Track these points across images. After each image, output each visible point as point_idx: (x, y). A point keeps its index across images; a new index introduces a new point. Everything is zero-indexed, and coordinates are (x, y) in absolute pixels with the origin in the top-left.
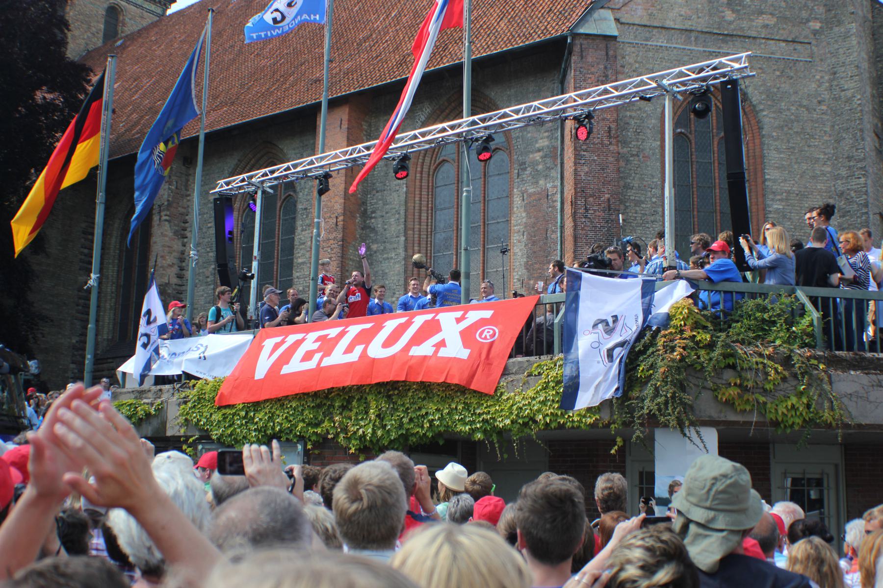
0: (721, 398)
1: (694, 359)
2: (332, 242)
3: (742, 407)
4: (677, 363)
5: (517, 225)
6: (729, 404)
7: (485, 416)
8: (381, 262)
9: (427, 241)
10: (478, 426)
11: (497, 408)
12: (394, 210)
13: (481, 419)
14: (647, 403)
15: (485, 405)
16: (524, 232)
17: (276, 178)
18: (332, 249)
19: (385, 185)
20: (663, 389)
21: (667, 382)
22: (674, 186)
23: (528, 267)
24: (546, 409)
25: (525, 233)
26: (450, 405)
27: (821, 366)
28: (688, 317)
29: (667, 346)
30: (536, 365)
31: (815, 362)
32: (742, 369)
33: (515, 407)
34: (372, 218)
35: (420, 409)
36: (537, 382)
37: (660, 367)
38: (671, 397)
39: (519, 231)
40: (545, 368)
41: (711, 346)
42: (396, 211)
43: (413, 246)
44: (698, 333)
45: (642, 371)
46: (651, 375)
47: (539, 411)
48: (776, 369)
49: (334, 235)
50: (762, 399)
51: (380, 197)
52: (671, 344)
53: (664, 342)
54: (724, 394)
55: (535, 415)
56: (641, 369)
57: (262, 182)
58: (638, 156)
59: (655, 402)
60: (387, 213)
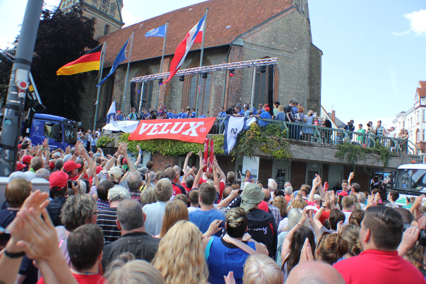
3: (266, 152)
6: (263, 151)
14: (242, 149)
17: (148, 79)
23: (214, 105)
27: (288, 143)
31: (286, 142)
35: (182, 145)
41: (260, 135)
48: (276, 143)
50: (272, 150)
57: (144, 80)
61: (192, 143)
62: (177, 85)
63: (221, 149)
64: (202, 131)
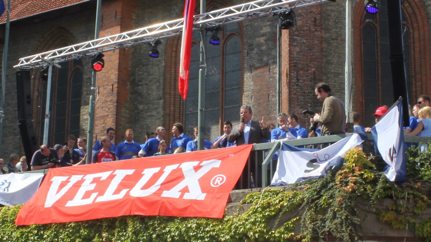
0: (382, 220)
1: (362, 191)
2: (109, 103)
3: (397, 226)
4: (349, 194)
5: (246, 91)
6: (389, 224)
7: (211, 233)
8: (146, 118)
9: (180, 103)
10: (206, 240)
11: (220, 227)
12: (156, 80)
13: (208, 235)
14: (328, 223)
15: (211, 225)
16: (252, 96)
17: (63, 57)
18: (109, 109)
19: (149, 61)
20: (339, 213)
21: (342, 208)
22: (352, 65)
24: (255, 228)
25: (253, 97)
26: (186, 225)
28: (358, 160)
29: (342, 181)
30: (248, 195)
32: (398, 198)
33: (233, 227)
34: (139, 85)
35: (164, 228)
36: (249, 208)
37: (338, 197)
38: (345, 219)
39: (248, 96)
40: (255, 197)
41: (374, 182)
42: (157, 80)
43: (170, 107)
44: (366, 172)
45: (325, 200)
46: (331, 203)
47: (250, 229)
48: (422, 199)
49: (111, 98)
50: (412, 220)
51: (145, 70)
52: (345, 180)
53: (341, 179)
54: (384, 217)
55: (247, 232)
56: (324, 198)
57: (53, 60)
58: (337, 40)
59: (334, 222)
60: (150, 81)
61: (191, 218)
62: (149, 75)
63: (270, 230)
64: (217, 184)
